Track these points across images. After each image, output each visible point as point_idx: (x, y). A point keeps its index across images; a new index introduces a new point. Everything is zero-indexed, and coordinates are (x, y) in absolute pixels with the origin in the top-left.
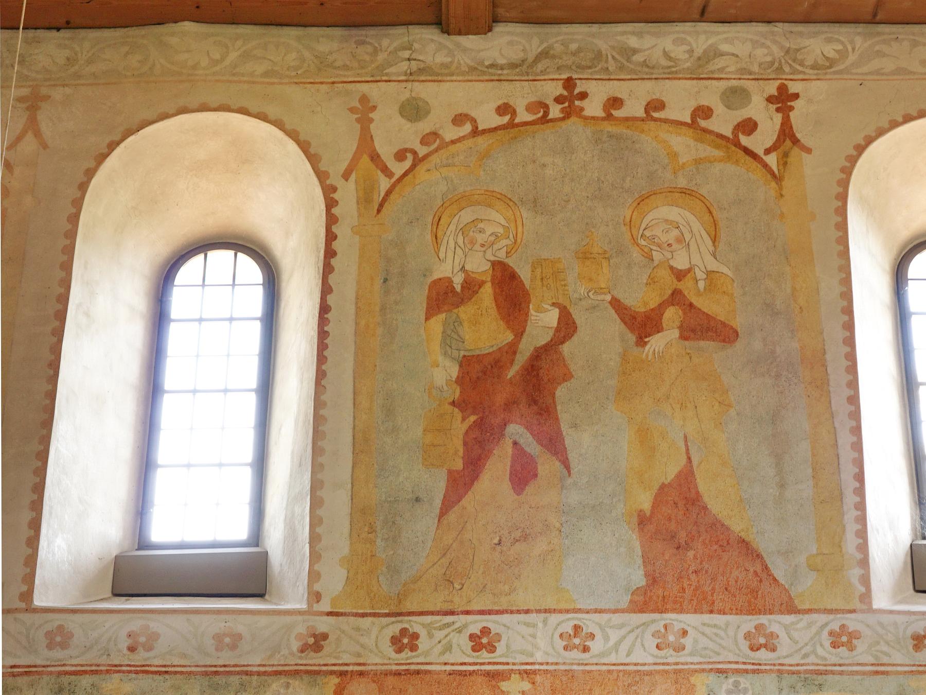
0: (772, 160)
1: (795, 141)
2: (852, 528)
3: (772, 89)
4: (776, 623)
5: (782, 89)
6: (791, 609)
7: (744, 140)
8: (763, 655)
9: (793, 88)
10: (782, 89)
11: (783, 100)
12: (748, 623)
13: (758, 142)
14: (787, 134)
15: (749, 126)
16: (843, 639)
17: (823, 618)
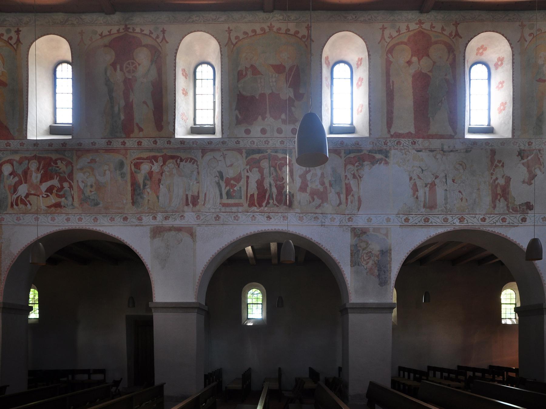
0: (15, 46)
1: (20, 42)
2: (25, 124)
3: (16, 29)
4: (11, 142)
5: (18, 29)
6: (14, 139)
7: (10, 41)
8: (8, 147)
9: (20, 29)
10: (18, 29)
11: (18, 32)
12: (6, 142)
13: (13, 42)
14: (18, 40)
15: (11, 38)
16: (22, 144)
17: (18, 141)
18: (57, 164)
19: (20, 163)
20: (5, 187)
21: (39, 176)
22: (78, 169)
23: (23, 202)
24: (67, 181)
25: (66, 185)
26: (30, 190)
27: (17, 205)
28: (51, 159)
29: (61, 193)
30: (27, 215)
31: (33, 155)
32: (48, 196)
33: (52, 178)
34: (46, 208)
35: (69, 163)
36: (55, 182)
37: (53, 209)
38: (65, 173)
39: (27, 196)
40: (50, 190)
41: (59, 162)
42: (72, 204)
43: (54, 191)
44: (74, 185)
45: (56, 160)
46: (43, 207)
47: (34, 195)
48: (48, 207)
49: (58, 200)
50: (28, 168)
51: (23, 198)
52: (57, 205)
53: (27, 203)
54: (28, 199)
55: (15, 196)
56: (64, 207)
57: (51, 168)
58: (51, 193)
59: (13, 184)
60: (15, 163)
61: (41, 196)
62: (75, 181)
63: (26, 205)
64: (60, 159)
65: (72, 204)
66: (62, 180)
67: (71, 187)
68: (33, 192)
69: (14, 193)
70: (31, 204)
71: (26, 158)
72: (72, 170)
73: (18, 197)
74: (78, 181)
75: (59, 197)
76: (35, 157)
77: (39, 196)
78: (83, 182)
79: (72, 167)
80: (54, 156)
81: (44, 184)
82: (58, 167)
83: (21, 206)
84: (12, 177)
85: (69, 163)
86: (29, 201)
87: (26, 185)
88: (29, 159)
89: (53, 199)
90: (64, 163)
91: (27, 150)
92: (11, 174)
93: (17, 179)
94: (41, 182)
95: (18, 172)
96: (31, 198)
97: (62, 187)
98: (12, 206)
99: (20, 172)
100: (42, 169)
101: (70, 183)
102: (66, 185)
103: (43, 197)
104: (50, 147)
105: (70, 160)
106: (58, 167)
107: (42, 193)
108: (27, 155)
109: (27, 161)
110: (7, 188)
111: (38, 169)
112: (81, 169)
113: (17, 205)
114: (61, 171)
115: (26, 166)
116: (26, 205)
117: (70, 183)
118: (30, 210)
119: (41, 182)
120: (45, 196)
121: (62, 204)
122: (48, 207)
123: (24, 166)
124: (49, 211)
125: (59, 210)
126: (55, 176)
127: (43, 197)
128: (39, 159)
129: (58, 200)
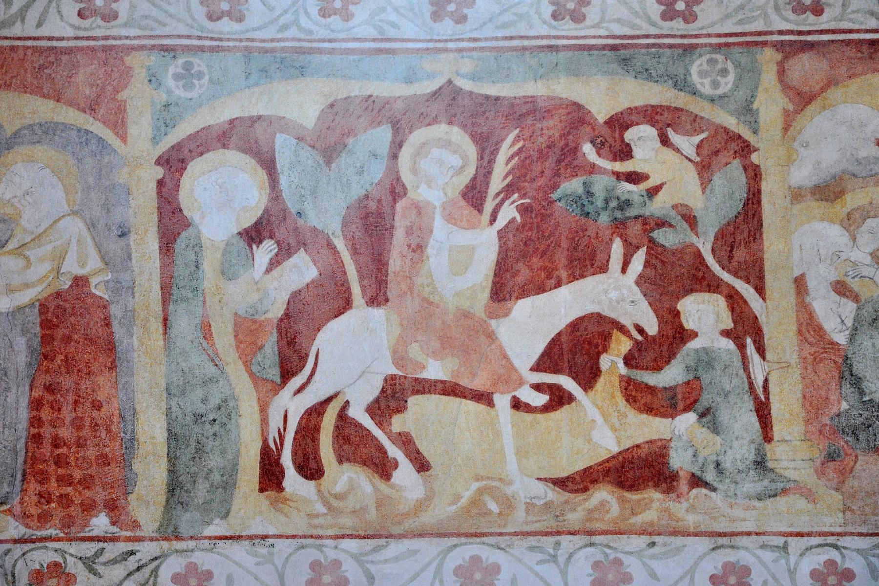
18: (625, 152)
19: (329, 145)
20: (206, 330)
21: (484, 245)
22: (797, 195)
23: (354, 444)
24: (713, 285)
25: (703, 313)
26: (415, 351)
27: (311, 469)
28: (578, 116)
29: (672, 375)
30: (395, 548)
31: (428, 87)
32: (559, 399)
33: (586, 262)
34: (552, 494)
35: (727, 148)
36: (616, 293)
37: (603, 494)
38: (691, 220)
39: (391, 399)
40: (576, 352)
41: (642, 136)
42: (760, 464)
43: (612, 363)
44: (774, 313)
45: (619, 123)
46: (528, 488)
47: (451, 389)
48: (561, 483)
49: (645, 429)
50: (396, 190)
51: (358, 413)
52: (641, 471)
53: (394, 452)
54: (398, 423)
55: (292, 404)
56: (697, 481)
57: (573, 186)
58: (588, 377)
59: (277, 311)
60: (284, 149)
61: (502, 401)
62: (778, 283)
63: (383, 468)
64: (652, 115)
65: (760, 464)
66: (673, 277)
67: (745, 329)
68: (435, 371)
69: (287, 375)
70: (422, 465)
71: (376, 110)
72: (754, 199)
73: (317, 411)
74: (800, 284)
75: (649, 410)
76: (450, 103)
77: (484, 398)
78: (841, 289)
79: (754, 174)
80: (603, 95)
81: (524, 308)
82: (634, 178)
83: (344, 477)
84: (265, 251)
85: (727, 148)
86: (406, 441)
87: (378, 313)
88: (401, 122)
89: (602, 425)
90: (687, 144)
91: (383, 49)
92: (254, 235)
93: (302, 270)
94: (503, 289)
95: (313, 219)
96: (421, 415)
97: (676, 335)
98: (271, 476)
99: (327, 213)
100: (509, 190)
101: (734, 299)
102: (703, 313)
103: (517, 404)
104: (568, 27)
105: (731, 122)
106: (634, 178)
107: (508, 376)
108: (387, 89)
109: (383, 135)
110: (224, 339)
111: (474, 194)
112: (829, 191)
113: (311, 469)
114: (659, 206)
115: (377, 172)
116: (383, 468)
117: (734, 299)
118: (421, 506)
119: (503, 289)
120: (540, 399)
121: (679, 460)
122: (561, 483)
123: (361, 170)
124: (574, 518)
125: (653, 503)
126: (617, 248)
127: (517, 404)
128: (483, 121)
129: (645, 429)
